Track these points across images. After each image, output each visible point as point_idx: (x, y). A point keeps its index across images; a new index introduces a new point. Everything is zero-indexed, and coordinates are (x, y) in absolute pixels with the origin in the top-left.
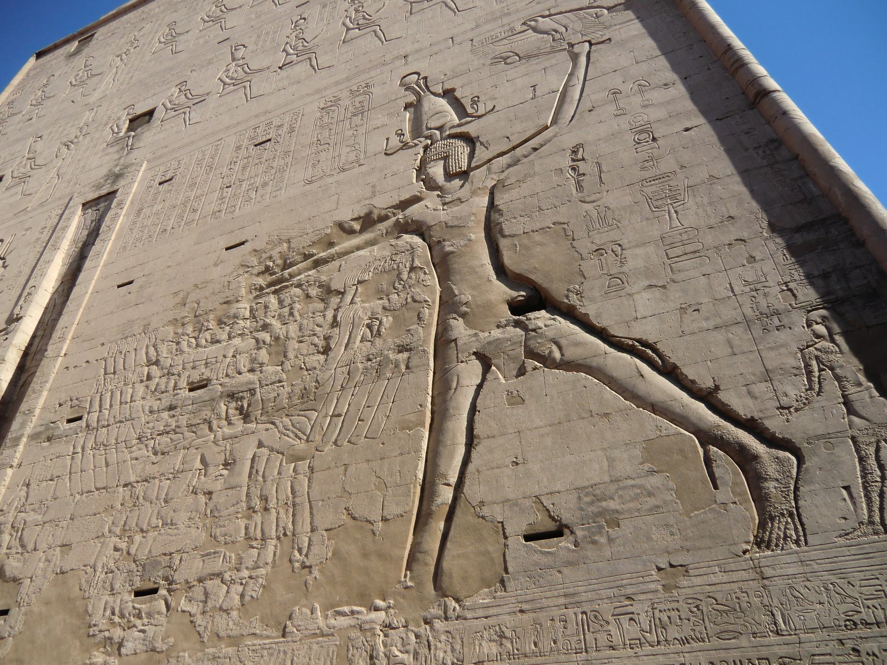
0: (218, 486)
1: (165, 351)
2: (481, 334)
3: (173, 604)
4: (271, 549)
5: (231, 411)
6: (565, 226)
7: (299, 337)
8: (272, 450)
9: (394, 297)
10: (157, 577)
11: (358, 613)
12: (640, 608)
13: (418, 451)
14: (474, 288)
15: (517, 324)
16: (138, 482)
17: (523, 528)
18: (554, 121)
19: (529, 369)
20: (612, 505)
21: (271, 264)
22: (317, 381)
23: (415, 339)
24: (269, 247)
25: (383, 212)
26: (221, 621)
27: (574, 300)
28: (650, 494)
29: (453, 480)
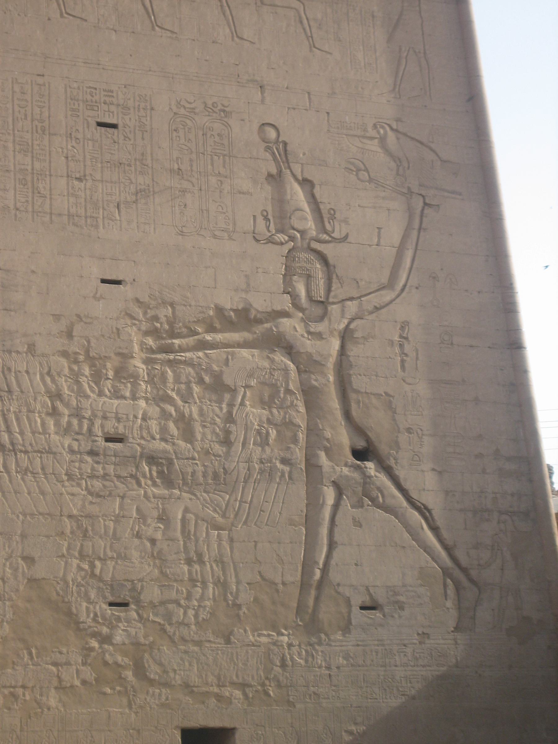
0: (159, 536)
1: (66, 388)
2: (336, 467)
3: (145, 616)
4: (211, 590)
5: (155, 474)
6: (391, 399)
7: (202, 421)
8: (197, 516)
9: (275, 411)
10: (125, 595)
11: (272, 635)
12: (409, 650)
13: (300, 543)
14: (333, 428)
15: (358, 468)
16: (82, 516)
17: (360, 603)
18: (390, 285)
19: (365, 504)
20: (402, 598)
21: (158, 325)
22: (224, 468)
23: (294, 457)
24: (153, 303)
25: (259, 316)
26: (184, 631)
27: (392, 462)
28: (419, 597)
29: (321, 566)
